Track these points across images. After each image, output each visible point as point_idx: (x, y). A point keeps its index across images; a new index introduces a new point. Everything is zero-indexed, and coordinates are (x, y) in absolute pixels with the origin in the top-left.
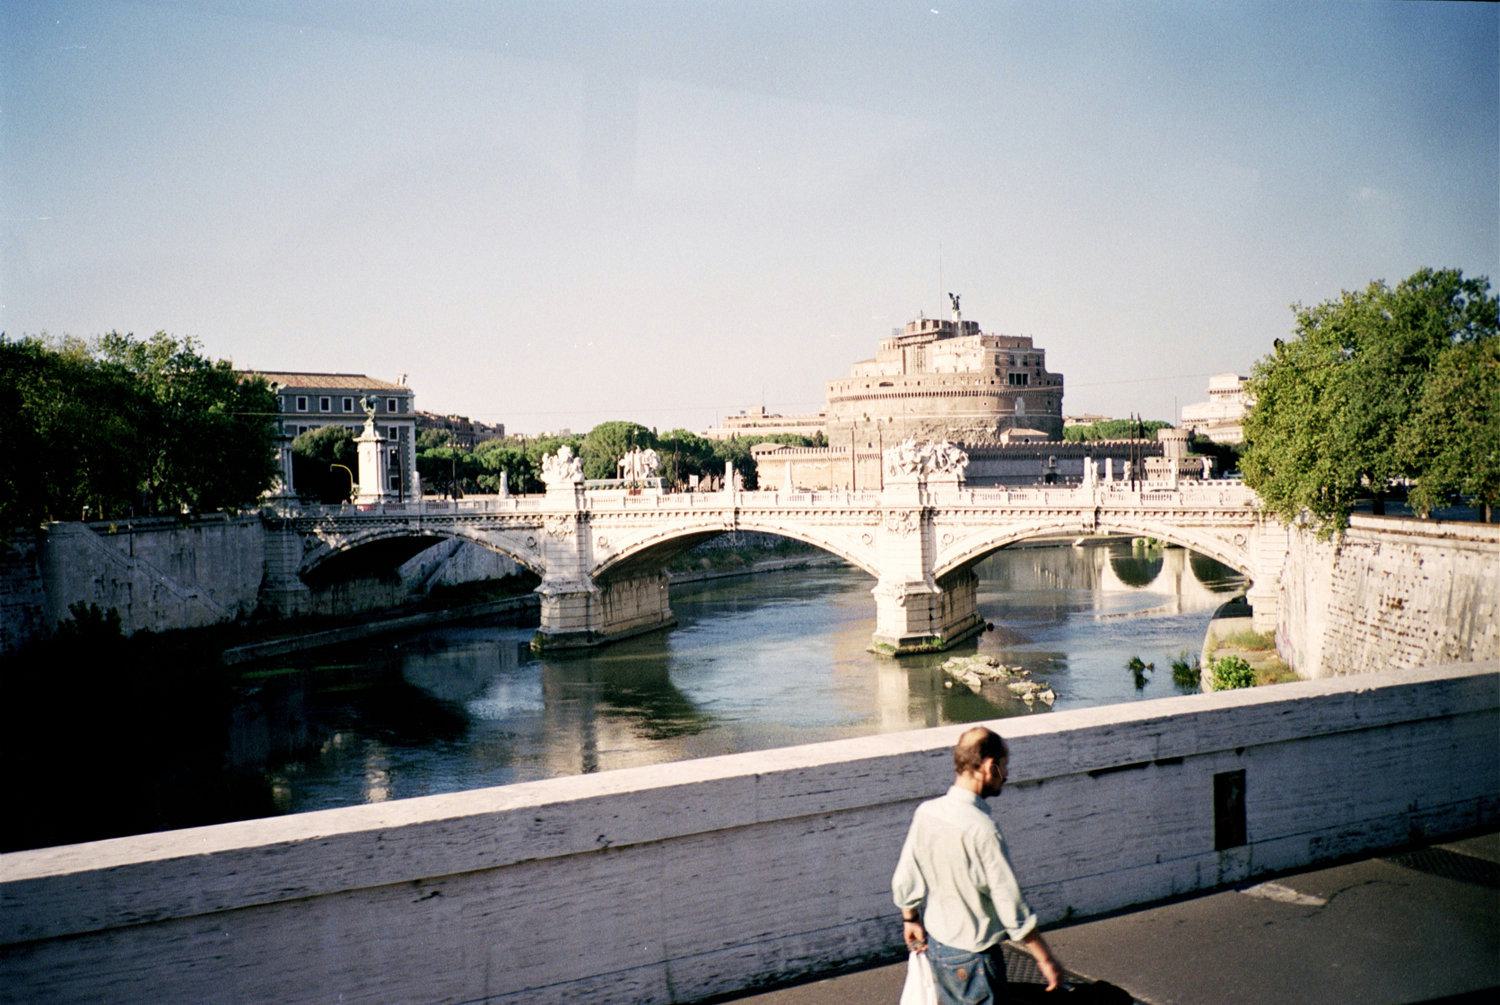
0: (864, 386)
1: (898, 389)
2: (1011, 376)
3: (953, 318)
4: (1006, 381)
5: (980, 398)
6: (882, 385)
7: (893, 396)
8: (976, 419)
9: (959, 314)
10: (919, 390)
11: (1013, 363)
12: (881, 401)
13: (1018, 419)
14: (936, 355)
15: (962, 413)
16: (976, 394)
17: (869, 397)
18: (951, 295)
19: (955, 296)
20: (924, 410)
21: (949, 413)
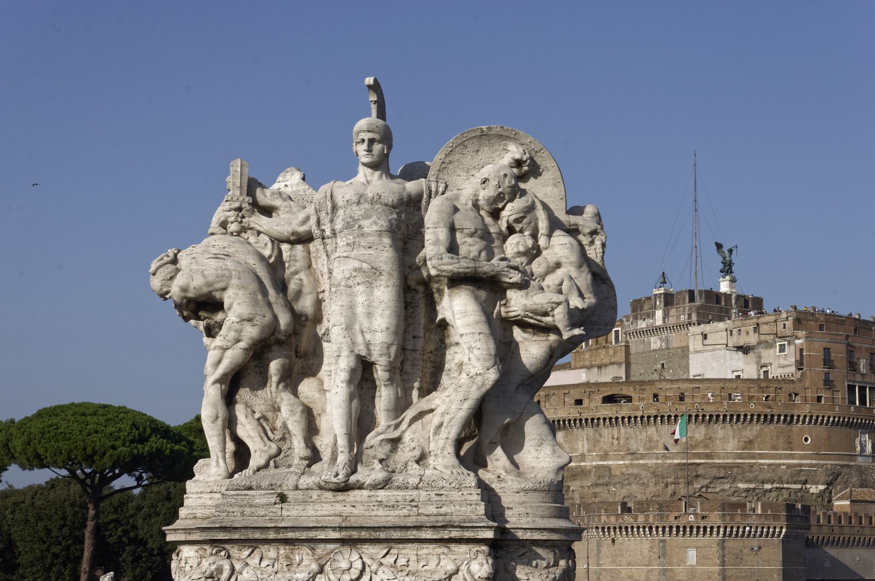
0: (570, 400)
1: (641, 406)
2: (851, 389)
3: (724, 287)
4: (841, 395)
5: (796, 427)
6: (610, 399)
7: (630, 420)
8: (789, 466)
9: (733, 281)
10: (682, 408)
11: (853, 366)
12: (607, 433)
13: (861, 470)
14: (697, 352)
15: (762, 456)
16: (789, 420)
17: (580, 423)
18: (719, 246)
19: (725, 250)
21: (740, 456)
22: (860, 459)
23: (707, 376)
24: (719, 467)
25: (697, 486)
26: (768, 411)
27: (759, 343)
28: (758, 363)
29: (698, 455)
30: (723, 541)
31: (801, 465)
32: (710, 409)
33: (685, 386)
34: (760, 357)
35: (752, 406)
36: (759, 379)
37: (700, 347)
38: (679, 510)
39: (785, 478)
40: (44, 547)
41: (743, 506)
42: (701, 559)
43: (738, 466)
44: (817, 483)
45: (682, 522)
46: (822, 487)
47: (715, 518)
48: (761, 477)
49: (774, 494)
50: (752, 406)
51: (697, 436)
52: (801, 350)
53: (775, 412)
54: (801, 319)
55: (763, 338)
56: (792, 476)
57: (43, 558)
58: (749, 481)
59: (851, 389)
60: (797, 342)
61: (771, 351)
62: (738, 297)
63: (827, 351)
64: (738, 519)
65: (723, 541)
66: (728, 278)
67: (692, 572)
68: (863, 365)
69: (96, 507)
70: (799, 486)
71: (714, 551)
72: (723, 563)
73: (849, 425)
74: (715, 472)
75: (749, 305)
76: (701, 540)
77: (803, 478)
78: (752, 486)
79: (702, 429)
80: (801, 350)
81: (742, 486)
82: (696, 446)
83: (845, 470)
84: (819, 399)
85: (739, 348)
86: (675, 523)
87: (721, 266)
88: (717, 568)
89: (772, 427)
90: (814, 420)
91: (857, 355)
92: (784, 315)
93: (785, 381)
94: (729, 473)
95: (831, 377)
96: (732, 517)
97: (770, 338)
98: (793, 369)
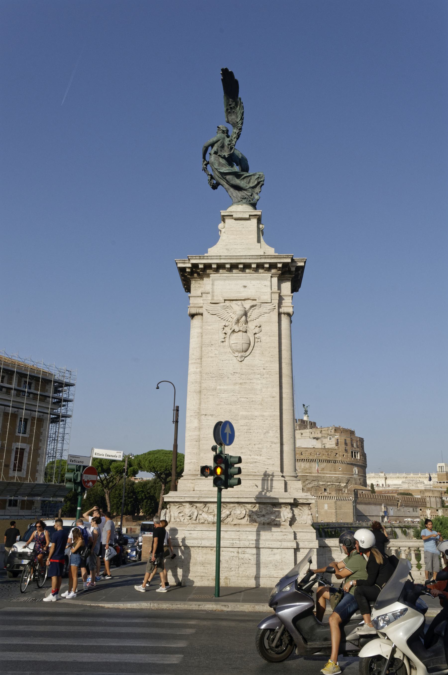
2: (352, 452)
3: (305, 418)
4: (350, 454)
5: (337, 464)
8: (335, 477)
9: (308, 416)
10: (302, 457)
11: (352, 445)
15: (327, 474)
16: (335, 462)
18: (304, 405)
19: (305, 406)
20: (305, 470)
22: (355, 475)
23: (303, 447)
24: (314, 477)
25: (307, 483)
26: (329, 459)
27: (322, 437)
28: (321, 443)
29: (307, 473)
30: (336, 502)
31: (339, 477)
32: (311, 458)
33: (303, 450)
34: (322, 441)
35: (324, 457)
36: (322, 448)
37: (300, 437)
38: (322, 491)
39: (334, 481)
40: (118, 500)
41: (342, 490)
42: (329, 507)
43: (320, 476)
44: (343, 483)
45: (323, 495)
46: (345, 484)
47: (334, 494)
48: (327, 480)
49: (330, 486)
50: (324, 457)
51: (306, 466)
52: (338, 440)
53: (331, 459)
54: (336, 430)
55: (323, 435)
56: (336, 480)
57: (117, 503)
58: (323, 482)
59: (352, 452)
60: (336, 437)
61: (326, 439)
62: (310, 422)
63: (345, 440)
64: (340, 494)
65: (336, 502)
66: (306, 415)
67: (326, 512)
68: (355, 445)
69: (165, 486)
70: (338, 484)
71: (333, 505)
72: (336, 509)
73: (352, 464)
74: (312, 478)
75: (313, 425)
76: (329, 501)
77: (339, 481)
78: (324, 483)
79: (308, 464)
80: (338, 440)
81: (321, 483)
82: (306, 469)
83: (351, 479)
84: (344, 455)
85: (314, 438)
86: (321, 495)
87: (304, 412)
88: (334, 511)
89: (330, 464)
90: (342, 462)
91: (353, 442)
92: (331, 428)
93: (332, 450)
94: (317, 479)
95: (347, 449)
96: (339, 493)
97: (326, 435)
98: (334, 446)
